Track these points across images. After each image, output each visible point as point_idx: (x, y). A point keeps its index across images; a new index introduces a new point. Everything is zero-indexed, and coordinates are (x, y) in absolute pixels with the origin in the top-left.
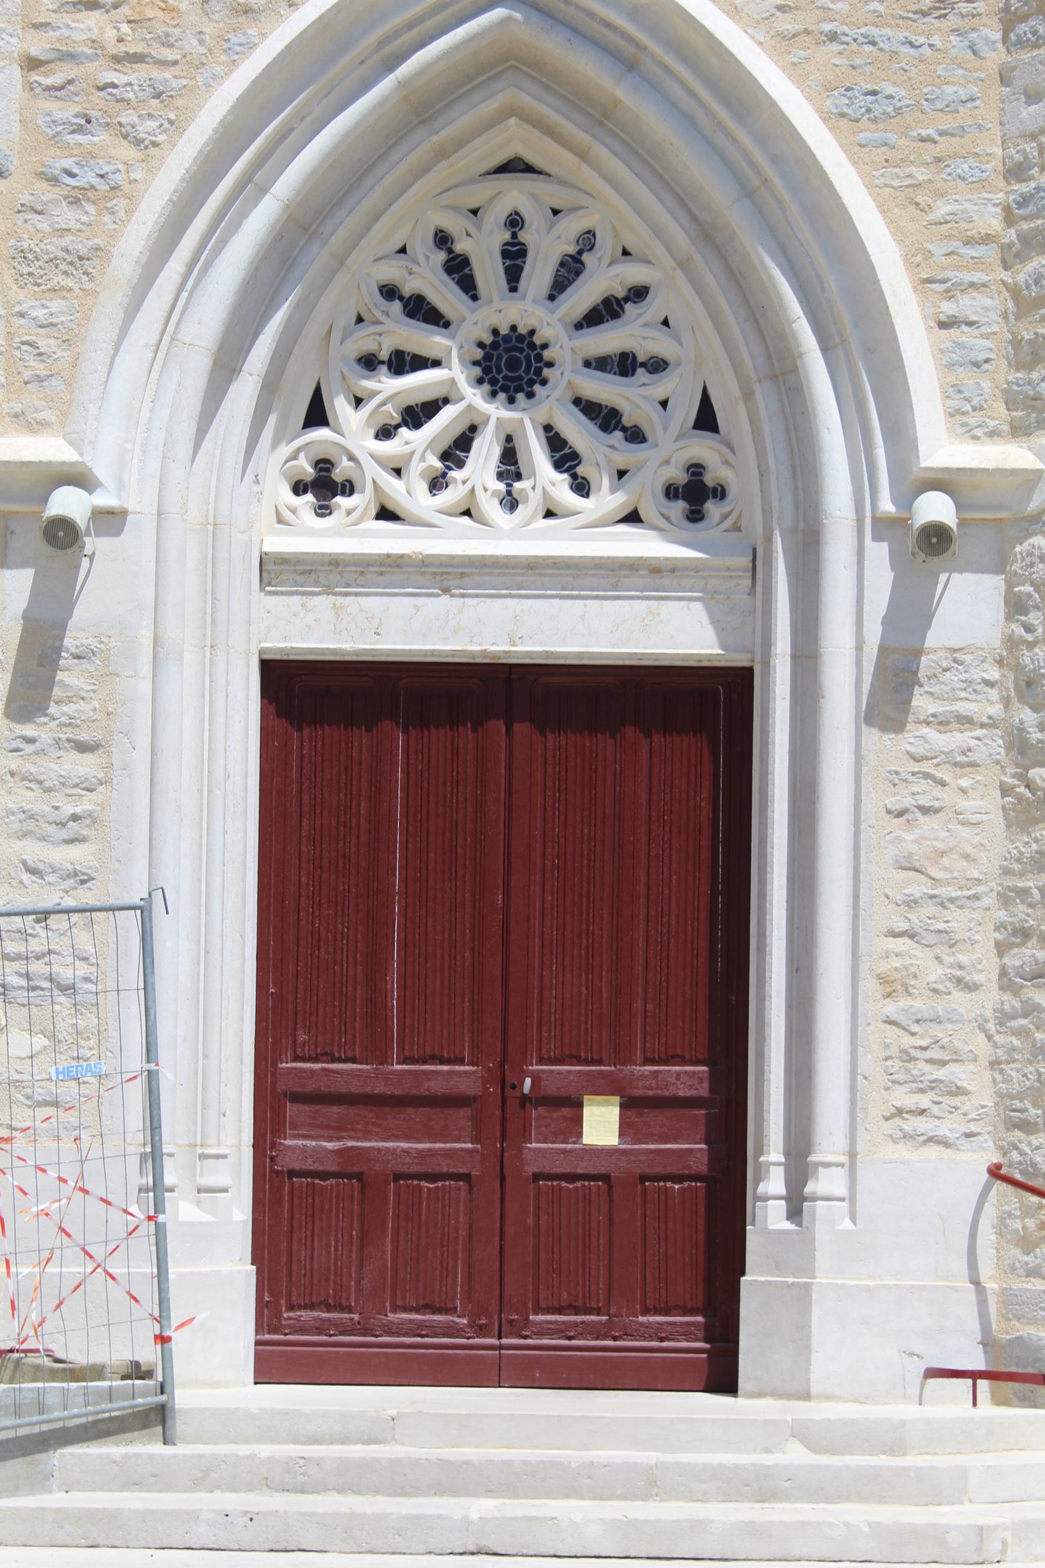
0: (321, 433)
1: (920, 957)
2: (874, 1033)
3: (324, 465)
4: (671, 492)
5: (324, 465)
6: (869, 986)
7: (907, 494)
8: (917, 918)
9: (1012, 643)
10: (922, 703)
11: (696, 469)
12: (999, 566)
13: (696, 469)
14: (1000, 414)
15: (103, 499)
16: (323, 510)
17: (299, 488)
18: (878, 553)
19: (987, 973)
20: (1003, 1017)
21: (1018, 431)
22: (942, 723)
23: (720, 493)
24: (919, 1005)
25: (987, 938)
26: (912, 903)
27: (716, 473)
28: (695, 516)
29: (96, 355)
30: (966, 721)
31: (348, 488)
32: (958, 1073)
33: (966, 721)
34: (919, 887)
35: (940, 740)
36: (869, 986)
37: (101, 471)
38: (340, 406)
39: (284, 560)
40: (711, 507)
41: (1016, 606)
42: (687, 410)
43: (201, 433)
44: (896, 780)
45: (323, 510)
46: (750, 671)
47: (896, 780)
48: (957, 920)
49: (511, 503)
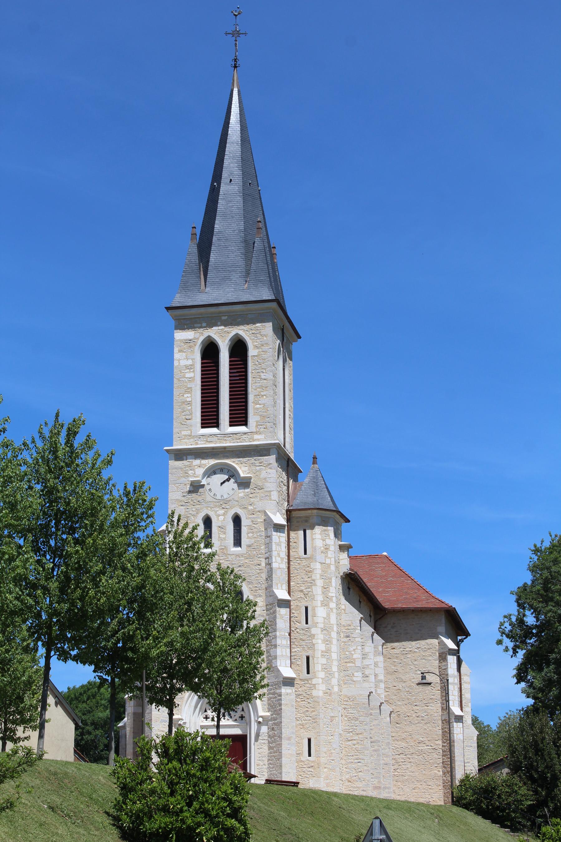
0: (206, 713)
1: (260, 762)
2: (256, 770)
3: (206, 716)
4: (240, 717)
5: (206, 716)
6: (256, 765)
7: (258, 719)
8: (260, 759)
9: (268, 732)
10: (260, 738)
11: (242, 715)
12: (267, 725)
13: (242, 715)
14: (267, 710)
15: (184, 721)
16: (206, 720)
17: (204, 718)
18: (256, 724)
19: (267, 764)
20: (268, 768)
21: (268, 711)
22: (262, 740)
23: (244, 717)
24: (260, 767)
25: (267, 760)
26: (260, 757)
27: (244, 715)
28: (242, 719)
29: (183, 708)
30: (264, 739)
31: (209, 718)
32: (264, 773)
33: (264, 739)
34: (260, 756)
35: (262, 741)
36: (256, 765)
37: (184, 718)
38: (208, 711)
39: (202, 726)
40: (243, 719)
41: (268, 728)
42: (241, 709)
43: (193, 714)
44: (258, 745)
45: (206, 720)
46: (246, 736)
47: (258, 745)
48: (264, 759)
49: (224, 719)
